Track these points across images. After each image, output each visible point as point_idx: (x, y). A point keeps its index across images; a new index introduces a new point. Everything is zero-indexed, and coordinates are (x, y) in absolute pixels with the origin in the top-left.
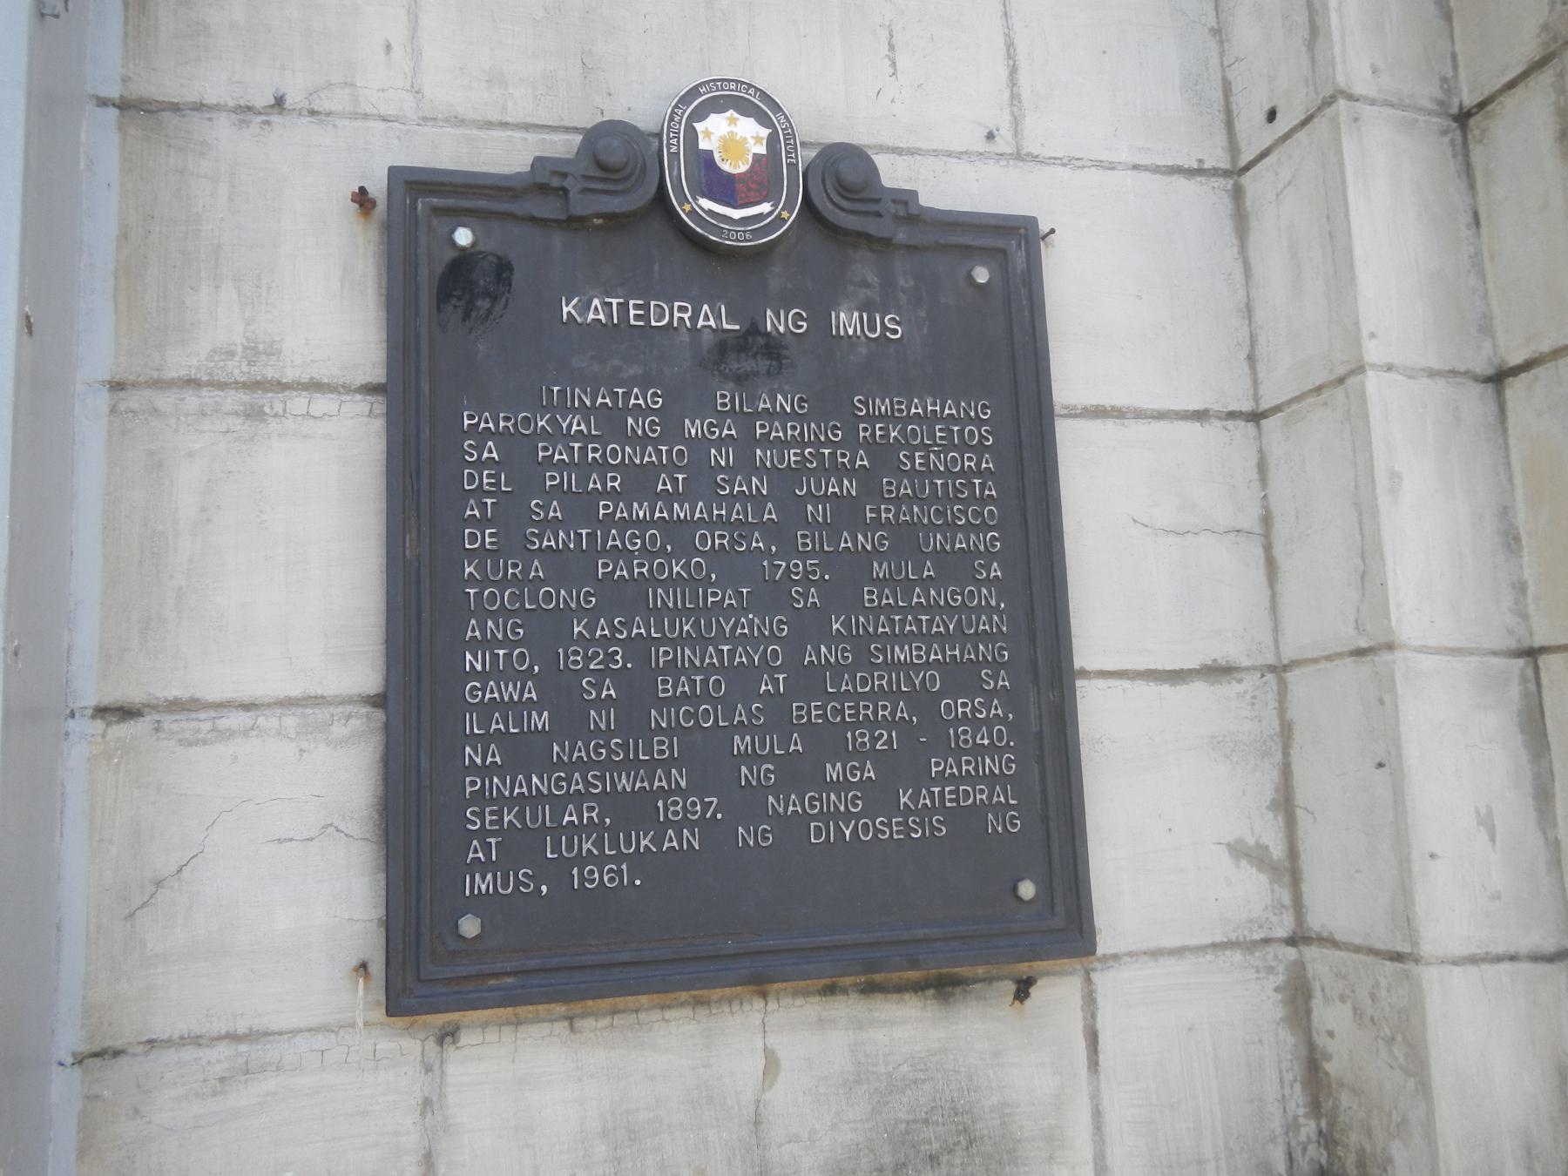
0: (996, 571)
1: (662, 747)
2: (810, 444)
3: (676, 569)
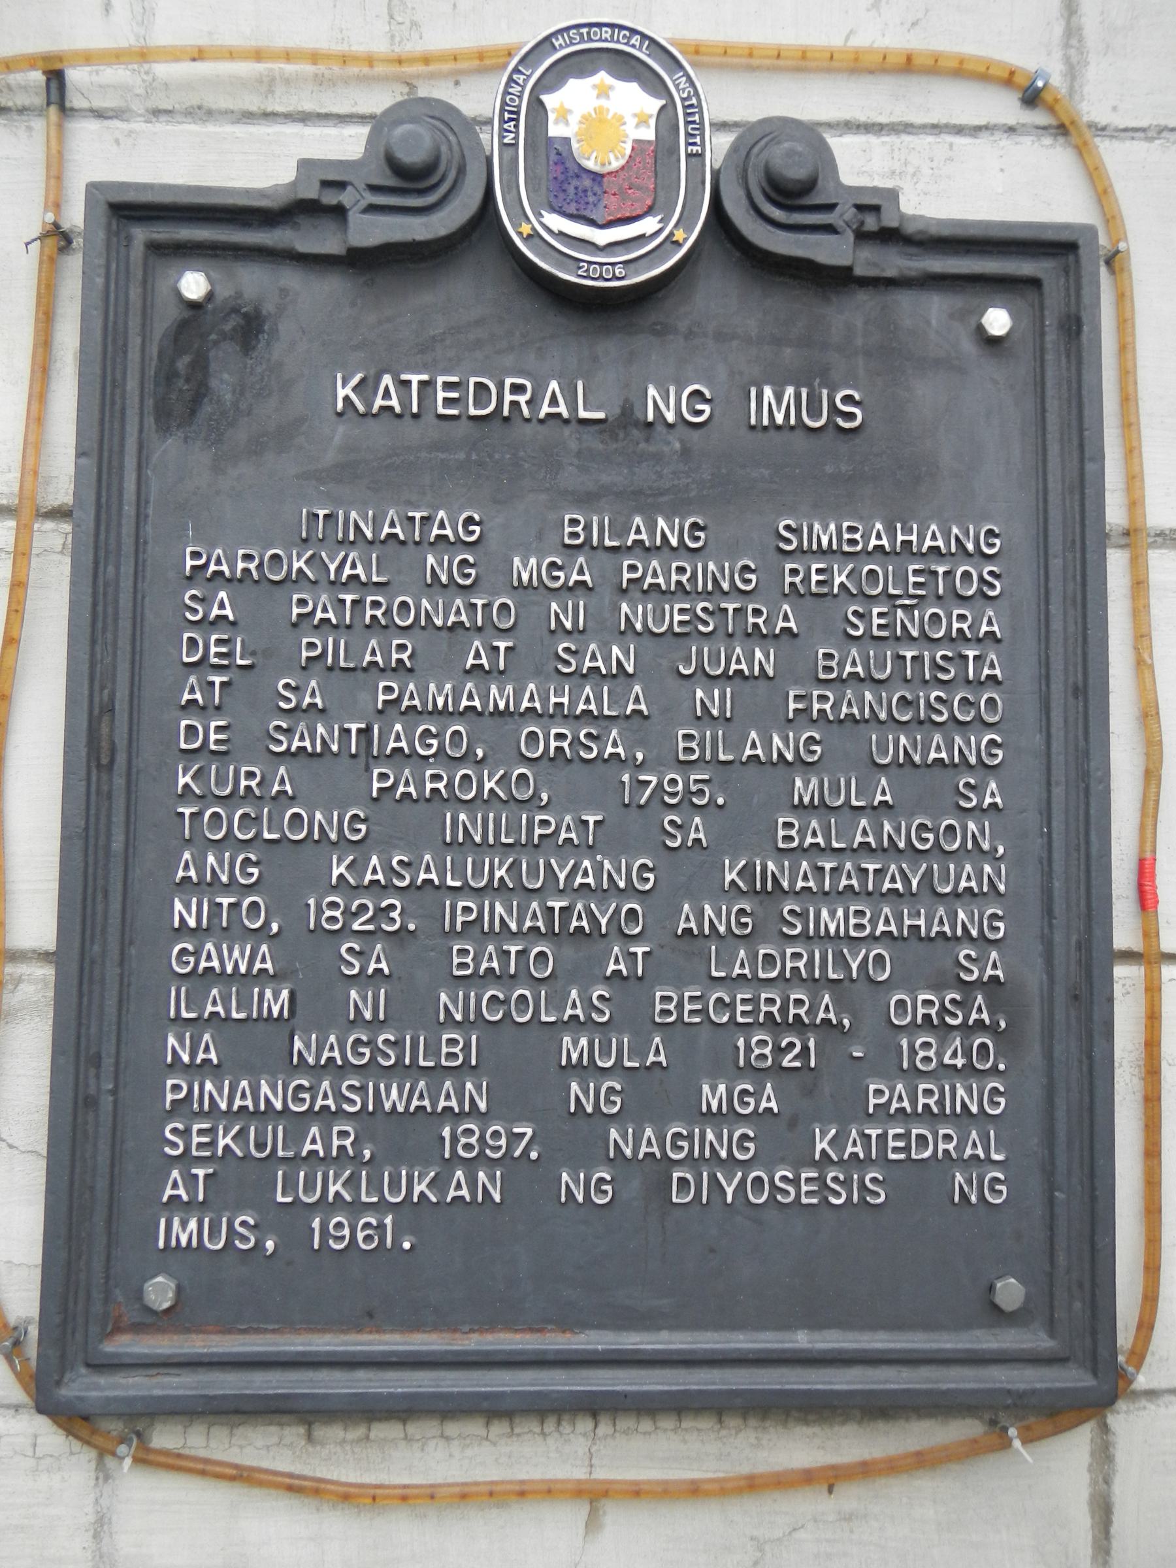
0: (992, 794)
1: (452, 1046)
2: (706, 595)
3: (488, 786)
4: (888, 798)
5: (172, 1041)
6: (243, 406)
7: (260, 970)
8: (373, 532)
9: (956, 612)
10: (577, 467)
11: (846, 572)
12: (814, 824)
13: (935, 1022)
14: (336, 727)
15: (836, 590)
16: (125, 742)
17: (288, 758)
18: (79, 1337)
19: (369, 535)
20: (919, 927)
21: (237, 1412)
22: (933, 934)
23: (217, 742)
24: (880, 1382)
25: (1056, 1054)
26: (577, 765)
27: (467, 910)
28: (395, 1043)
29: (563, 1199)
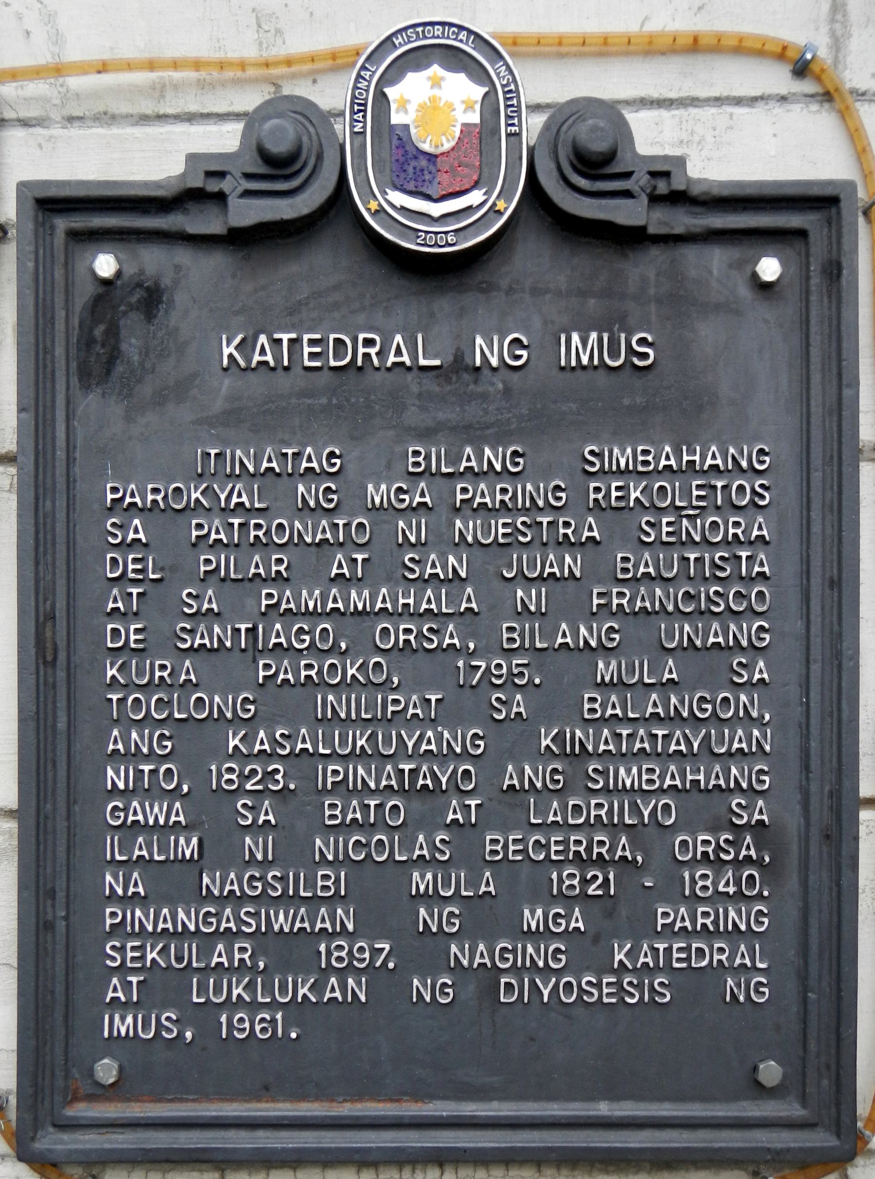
0: (761, 671)
1: (326, 880)
2: (525, 511)
3: (350, 672)
4: (674, 676)
5: (109, 878)
6: (148, 366)
7: (175, 822)
8: (255, 467)
9: (732, 520)
10: (418, 407)
11: (640, 489)
12: (614, 698)
13: (712, 857)
14: (229, 627)
15: (632, 504)
16: (65, 643)
17: (192, 653)
18: (47, 1104)
19: (251, 469)
20: (699, 781)
21: (167, 1161)
22: (710, 787)
23: (136, 641)
24: (666, 1142)
25: (811, 882)
26: (421, 654)
27: (335, 772)
28: (281, 878)
29: (415, 1000)
